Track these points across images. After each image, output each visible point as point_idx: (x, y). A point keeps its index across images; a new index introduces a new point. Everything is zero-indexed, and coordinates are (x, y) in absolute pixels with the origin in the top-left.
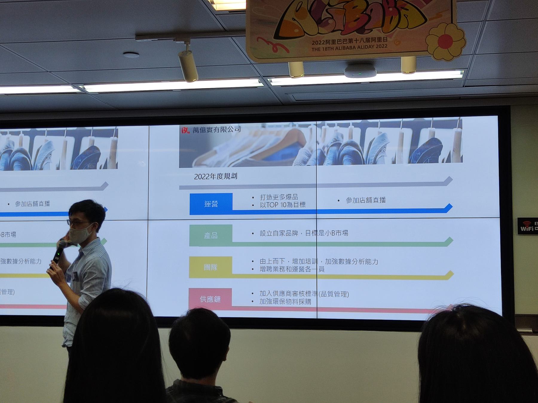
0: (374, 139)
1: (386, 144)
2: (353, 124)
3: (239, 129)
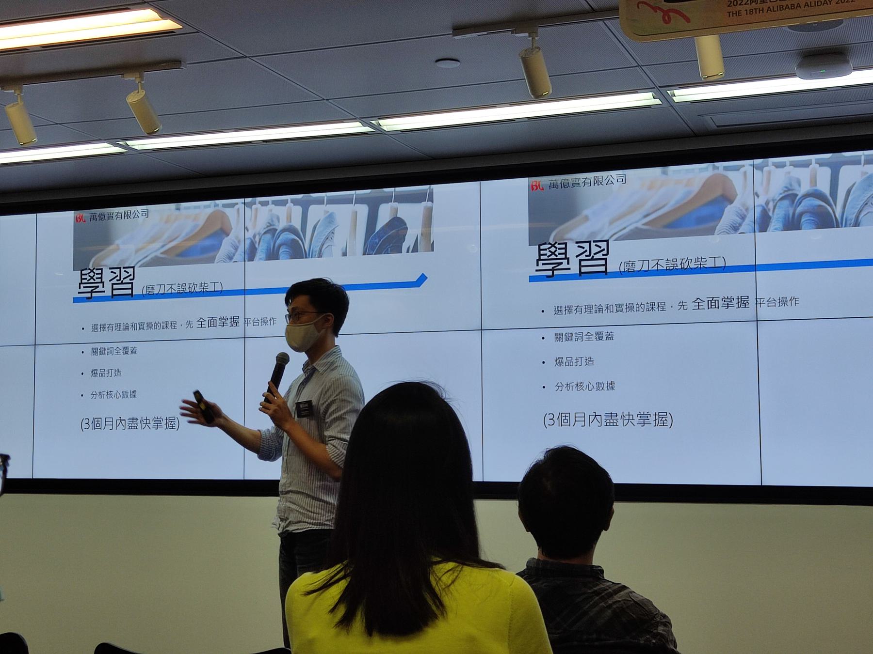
0: (319, 221)
1: (334, 229)
2: (293, 201)
3: (147, 214)
